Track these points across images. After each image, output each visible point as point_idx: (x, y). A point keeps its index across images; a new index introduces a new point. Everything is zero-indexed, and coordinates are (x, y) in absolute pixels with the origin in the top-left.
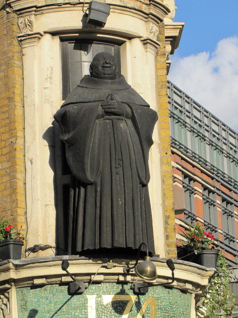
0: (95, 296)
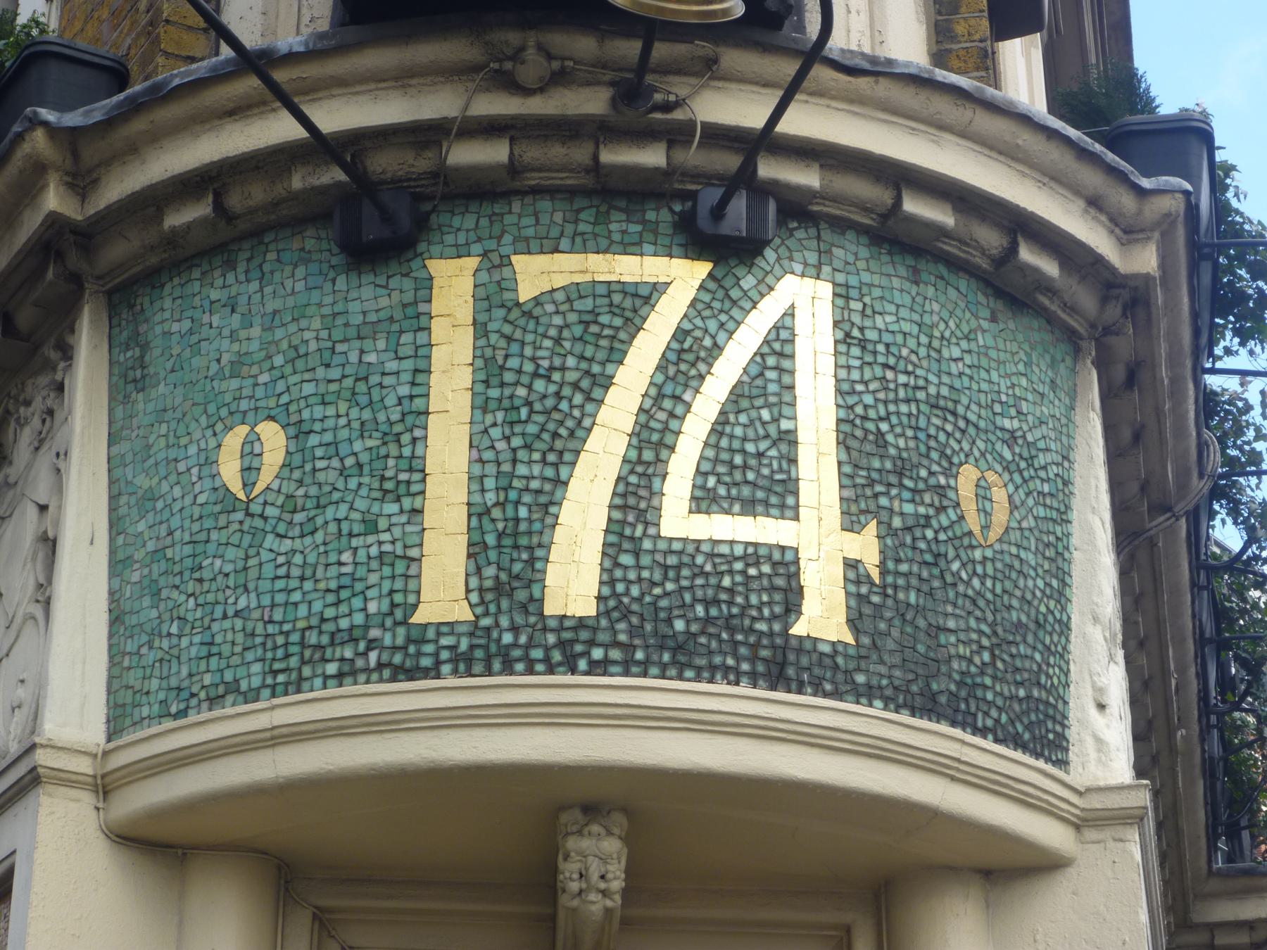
0: (472, 263)
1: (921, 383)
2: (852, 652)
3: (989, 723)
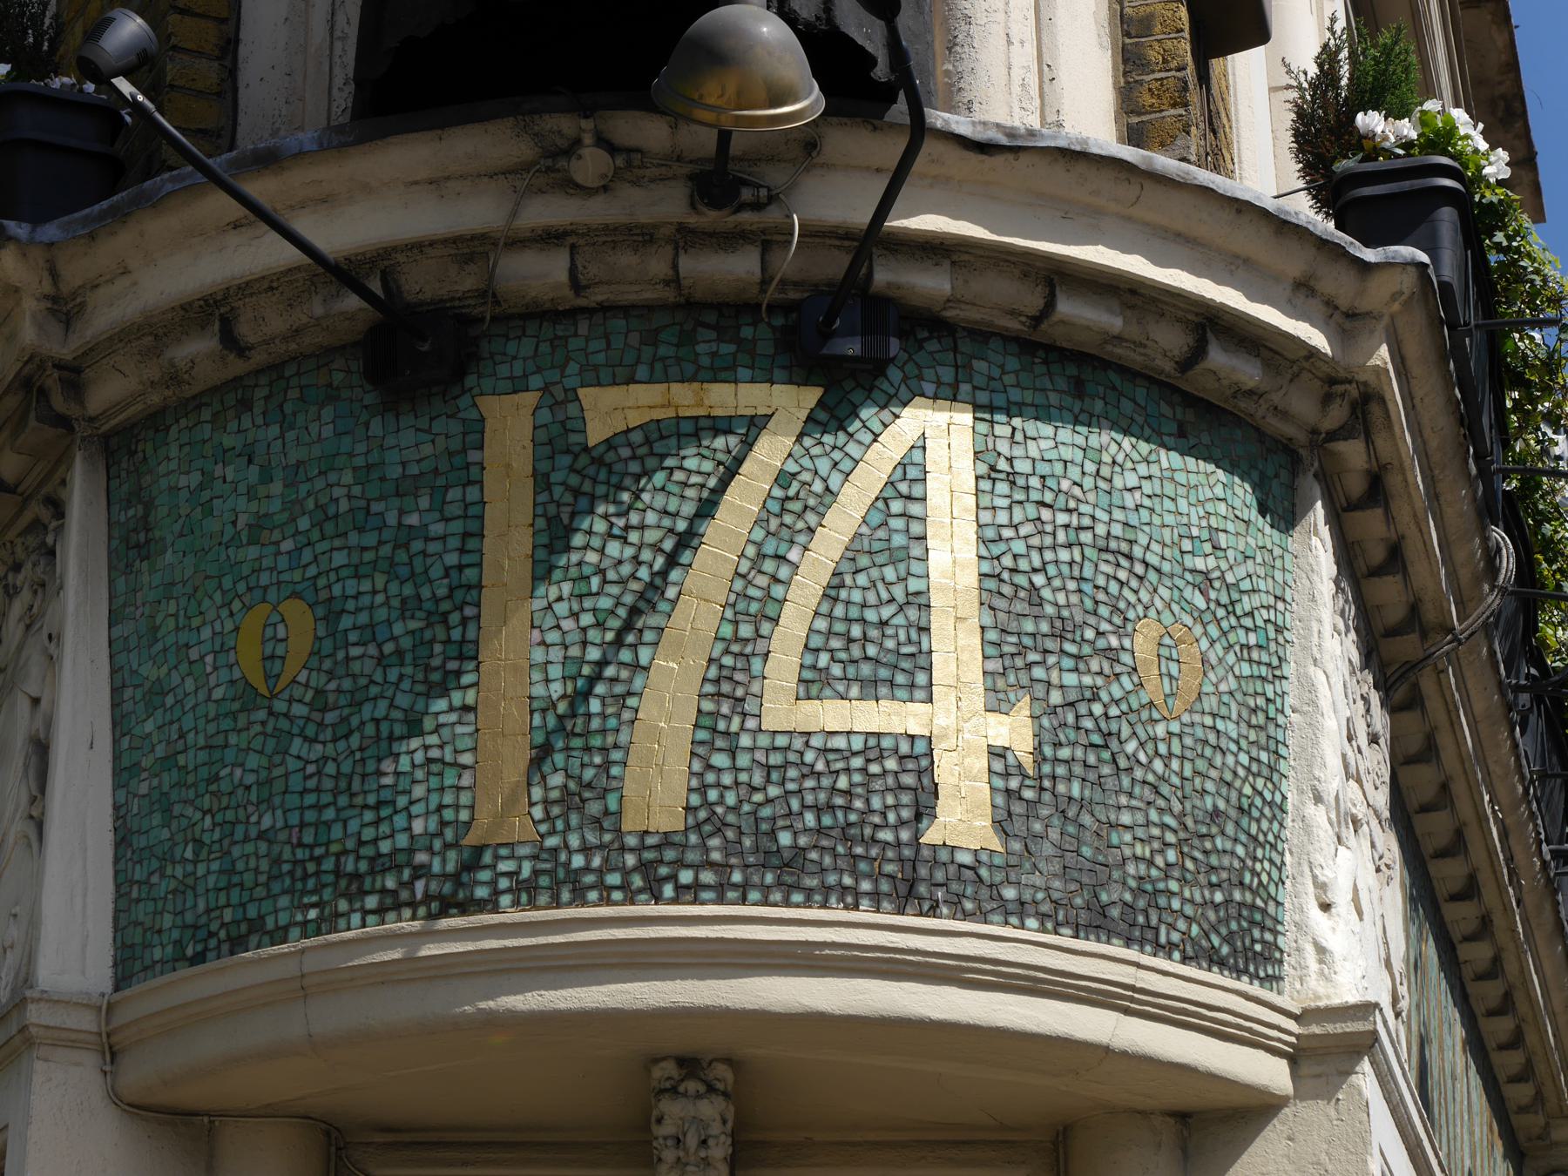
0: (530, 399)
1: (1086, 521)
2: (998, 861)
3: (1175, 937)
